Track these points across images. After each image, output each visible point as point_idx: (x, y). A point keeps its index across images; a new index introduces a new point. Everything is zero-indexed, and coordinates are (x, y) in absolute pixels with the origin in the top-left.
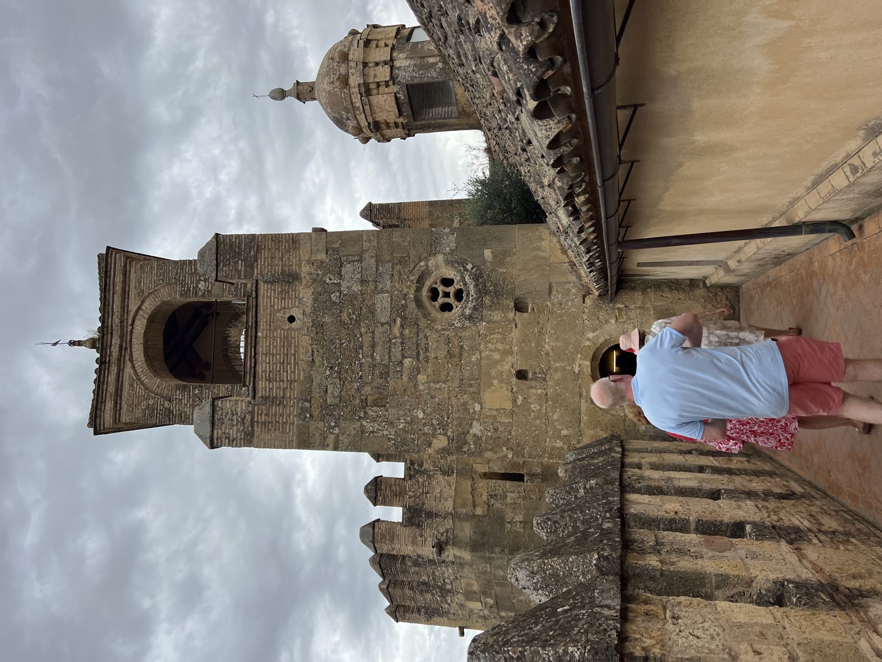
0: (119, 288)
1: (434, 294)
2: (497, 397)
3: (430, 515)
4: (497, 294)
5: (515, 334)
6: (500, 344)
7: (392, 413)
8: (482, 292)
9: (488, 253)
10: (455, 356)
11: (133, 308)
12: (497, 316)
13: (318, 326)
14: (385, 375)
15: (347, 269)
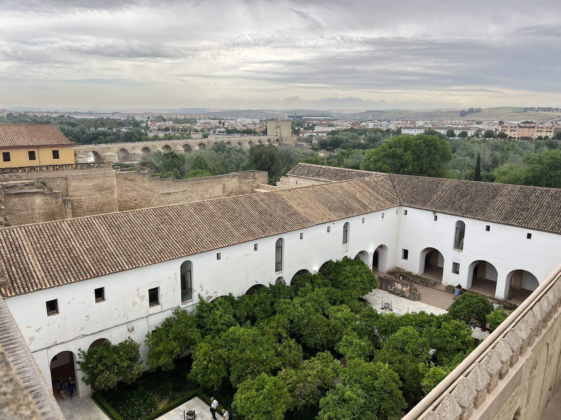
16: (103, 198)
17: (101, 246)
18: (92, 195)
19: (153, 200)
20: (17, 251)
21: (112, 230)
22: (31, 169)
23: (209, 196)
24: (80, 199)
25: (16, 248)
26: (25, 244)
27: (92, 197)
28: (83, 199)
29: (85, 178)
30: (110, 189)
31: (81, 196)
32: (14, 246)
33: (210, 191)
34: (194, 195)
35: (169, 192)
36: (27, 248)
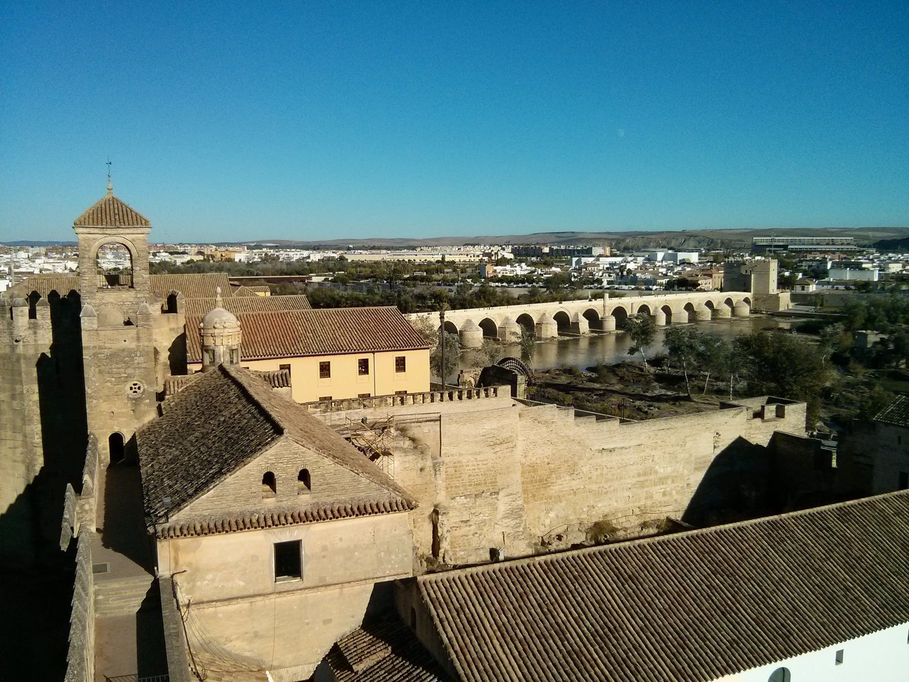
0: (136, 232)
1: (135, 385)
2: (105, 406)
3: (35, 333)
4: (135, 404)
5: (124, 410)
6: (122, 407)
7: (97, 375)
8: (135, 399)
9: (148, 401)
10: (117, 394)
11: (127, 237)
12: (129, 405)
13: (123, 350)
14: (109, 373)
15: (142, 358)
16: (498, 461)
17: (615, 628)
18: (479, 453)
19: (581, 463)
20: (473, 630)
21: (623, 585)
22: (381, 401)
23: (687, 456)
24: (459, 462)
25: (469, 622)
26: (482, 614)
27: (478, 457)
28: (464, 460)
29: (469, 418)
30: (507, 442)
31: (460, 455)
32: (462, 616)
33: (689, 445)
34: (658, 453)
35: (611, 446)
36: (487, 625)
